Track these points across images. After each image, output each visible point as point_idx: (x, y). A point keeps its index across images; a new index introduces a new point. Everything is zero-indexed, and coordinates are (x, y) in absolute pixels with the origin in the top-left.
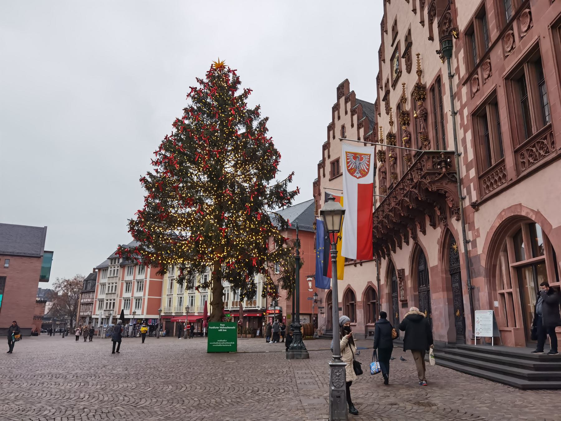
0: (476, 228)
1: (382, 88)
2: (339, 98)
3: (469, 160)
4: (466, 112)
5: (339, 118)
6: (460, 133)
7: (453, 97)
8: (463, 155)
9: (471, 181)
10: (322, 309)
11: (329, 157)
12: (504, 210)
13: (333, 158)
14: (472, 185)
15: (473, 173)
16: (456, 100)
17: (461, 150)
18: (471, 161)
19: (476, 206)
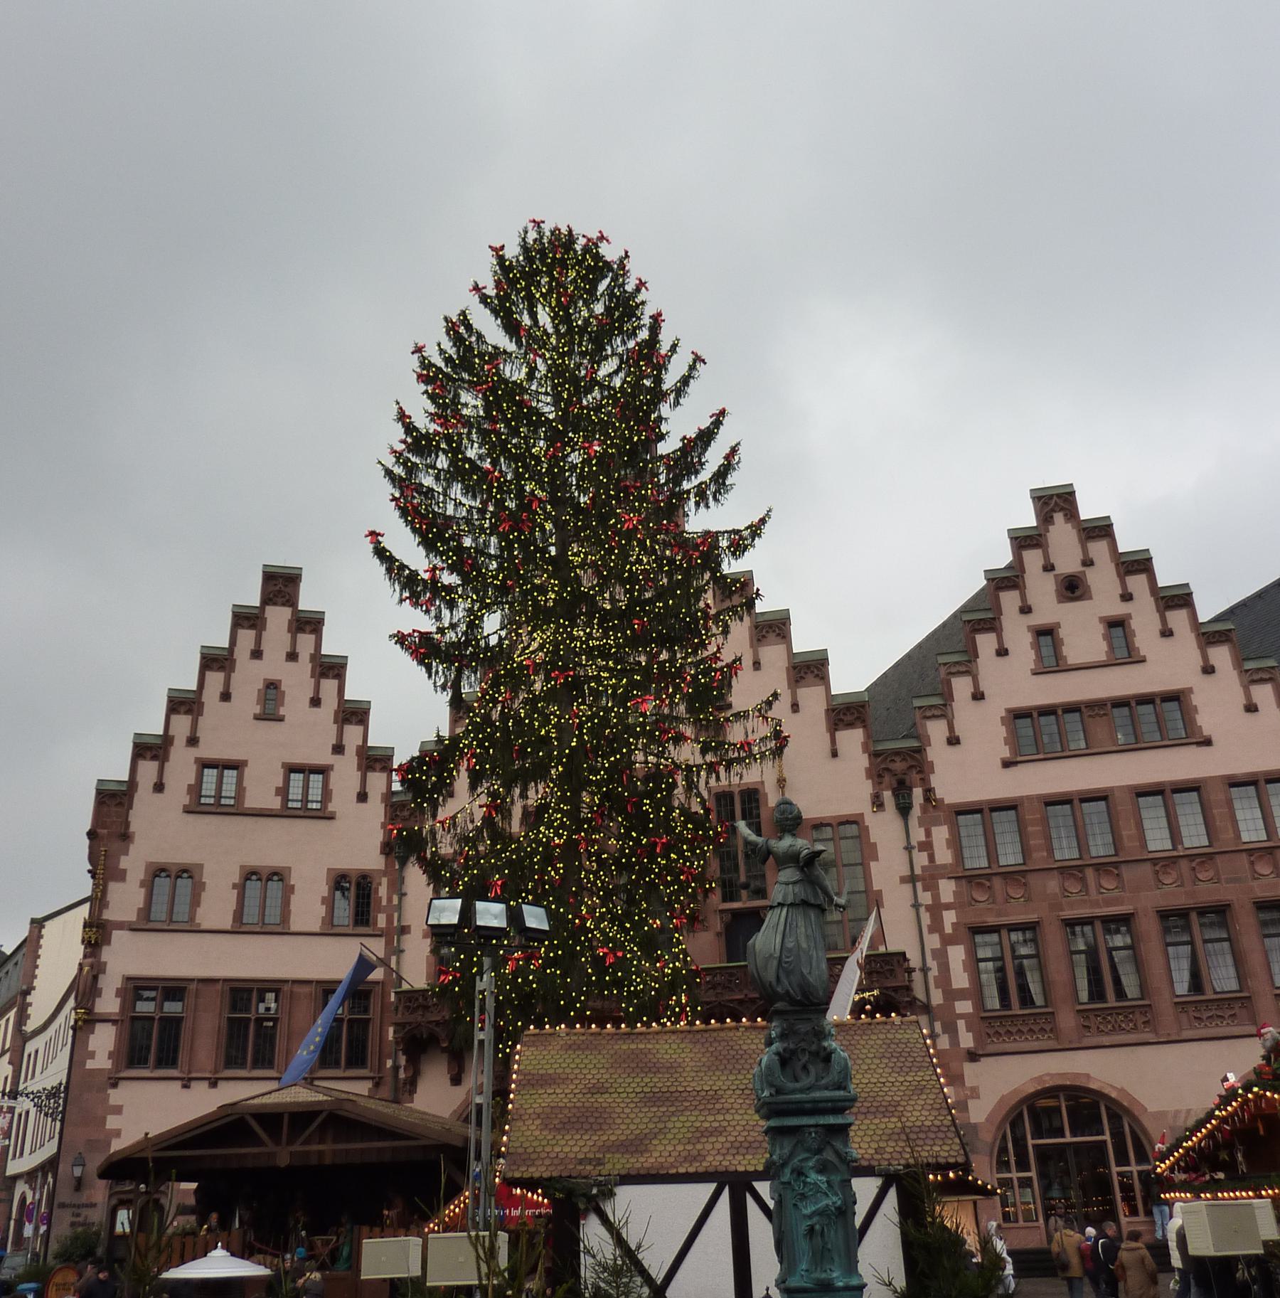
0: (968, 1084)
2: (268, 598)
3: (955, 986)
4: (949, 917)
5: (257, 654)
7: (911, 879)
8: (934, 972)
9: (961, 1016)
10: (84, 1212)
11: (193, 741)
12: (1048, 1074)
13: (207, 750)
14: (961, 1024)
15: (964, 1007)
16: (919, 885)
17: (932, 964)
18: (962, 990)
19: (973, 1056)
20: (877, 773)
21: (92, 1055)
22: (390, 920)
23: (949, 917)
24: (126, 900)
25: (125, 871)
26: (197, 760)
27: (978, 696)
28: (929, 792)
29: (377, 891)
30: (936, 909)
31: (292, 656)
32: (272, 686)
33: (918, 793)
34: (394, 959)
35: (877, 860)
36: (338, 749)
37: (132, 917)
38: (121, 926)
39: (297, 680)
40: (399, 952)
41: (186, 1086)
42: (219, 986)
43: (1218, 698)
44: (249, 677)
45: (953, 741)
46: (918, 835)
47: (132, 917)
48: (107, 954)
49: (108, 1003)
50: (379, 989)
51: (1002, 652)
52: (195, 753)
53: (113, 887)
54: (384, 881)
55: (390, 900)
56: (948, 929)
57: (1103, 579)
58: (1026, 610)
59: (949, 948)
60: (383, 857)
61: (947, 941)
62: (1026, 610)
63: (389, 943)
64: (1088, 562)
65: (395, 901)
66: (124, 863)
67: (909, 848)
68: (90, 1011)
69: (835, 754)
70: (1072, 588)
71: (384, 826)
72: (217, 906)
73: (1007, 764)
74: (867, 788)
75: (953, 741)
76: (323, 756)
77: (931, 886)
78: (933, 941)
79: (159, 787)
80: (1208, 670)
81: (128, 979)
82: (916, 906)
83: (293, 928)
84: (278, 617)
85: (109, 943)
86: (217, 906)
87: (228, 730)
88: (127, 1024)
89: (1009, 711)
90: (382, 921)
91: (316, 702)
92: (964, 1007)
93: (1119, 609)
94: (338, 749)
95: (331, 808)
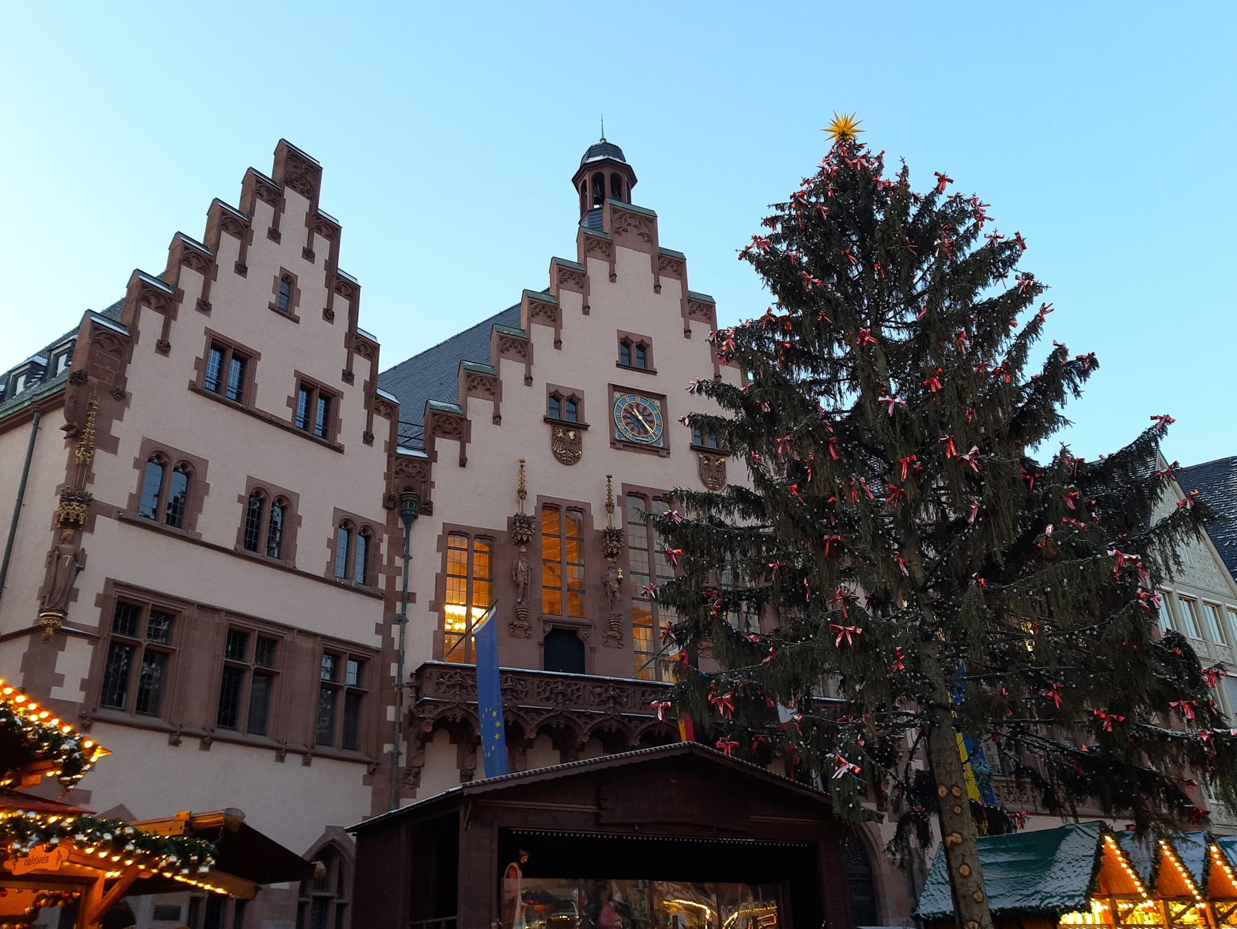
1: (528, 380)
11: (204, 306)
21: (59, 680)
22: (391, 582)
24: (116, 479)
25: (116, 441)
26: (208, 332)
29: (378, 547)
31: (308, 254)
34: (395, 629)
36: (348, 376)
37: (123, 505)
38: (108, 511)
39: (311, 282)
40: (402, 620)
44: (267, 259)
47: (123, 505)
49: (86, 612)
50: (376, 660)
52: (202, 321)
53: (101, 458)
54: (386, 537)
55: (391, 560)
60: (384, 512)
63: (389, 608)
65: (399, 562)
66: (117, 428)
71: (387, 477)
76: (333, 379)
79: (163, 347)
81: (113, 584)
83: (300, 566)
84: (295, 202)
85: (91, 530)
86: (221, 517)
87: (241, 309)
88: (104, 646)
90: (382, 583)
94: (348, 376)
95: (340, 439)
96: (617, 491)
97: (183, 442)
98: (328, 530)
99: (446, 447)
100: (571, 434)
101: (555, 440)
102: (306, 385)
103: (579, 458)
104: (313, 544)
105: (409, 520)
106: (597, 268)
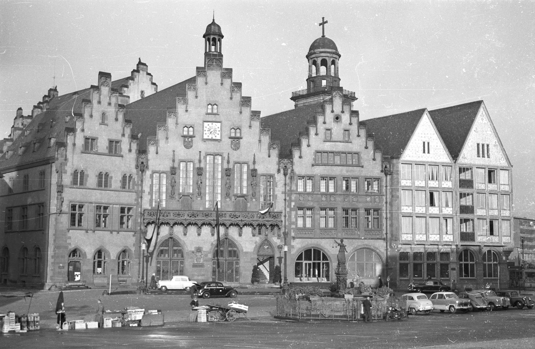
4: (293, 204)
6: (288, 210)
7: (285, 193)
9: (293, 228)
11: (83, 130)
20: (279, 163)
23: (293, 204)
24: (67, 179)
27: (309, 146)
28: (293, 170)
30: (291, 201)
31: (110, 104)
32: (104, 114)
33: (289, 171)
35: (277, 187)
36: (123, 135)
38: (67, 186)
41: (87, 232)
42: (94, 205)
43: (368, 154)
45: (300, 157)
46: (288, 181)
48: (64, 195)
49: (66, 208)
51: (317, 134)
53: (64, 176)
56: (292, 207)
57: (345, 118)
58: (324, 123)
59: (292, 212)
61: (291, 209)
62: (324, 123)
63: (137, 195)
64: (343, 112)
65: (140, 182)
66: (66, 168)
67: (285, 184)
68: (61, 211)
69: (269, 157)
70: (337, 118)
72: (92, 180)
73: (313, 165)
74: (277, 167)
75: (300, 157)
77: (290, 196)
78: (288, 210)
80: (366, 148)
82: (285, 200)
86: (92, 180)
89: (316, 151)
91: (117, 120)
92: (293, 226)
93: (348, 127)
94: (123, 135)
96: (203, 154)
97: (81, 166)
98: (120, 178)
99: (152, 149)
100: (190, 140)
101: (185, 141)
102: (111, 142)
103: (192, 146)
104: (116, 182)
105: (143, 171)
106: (200, 81)
